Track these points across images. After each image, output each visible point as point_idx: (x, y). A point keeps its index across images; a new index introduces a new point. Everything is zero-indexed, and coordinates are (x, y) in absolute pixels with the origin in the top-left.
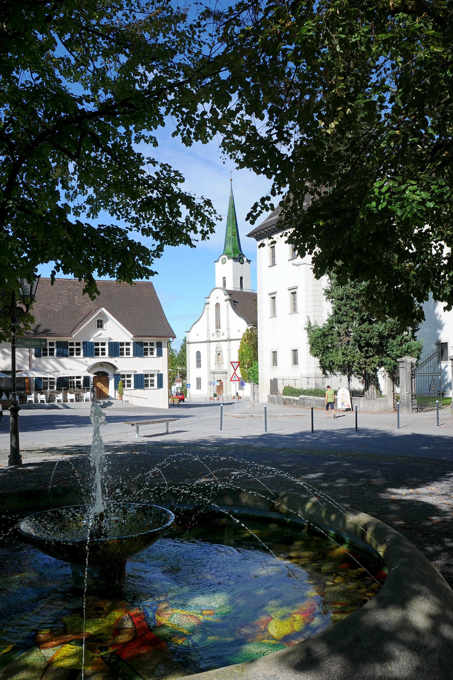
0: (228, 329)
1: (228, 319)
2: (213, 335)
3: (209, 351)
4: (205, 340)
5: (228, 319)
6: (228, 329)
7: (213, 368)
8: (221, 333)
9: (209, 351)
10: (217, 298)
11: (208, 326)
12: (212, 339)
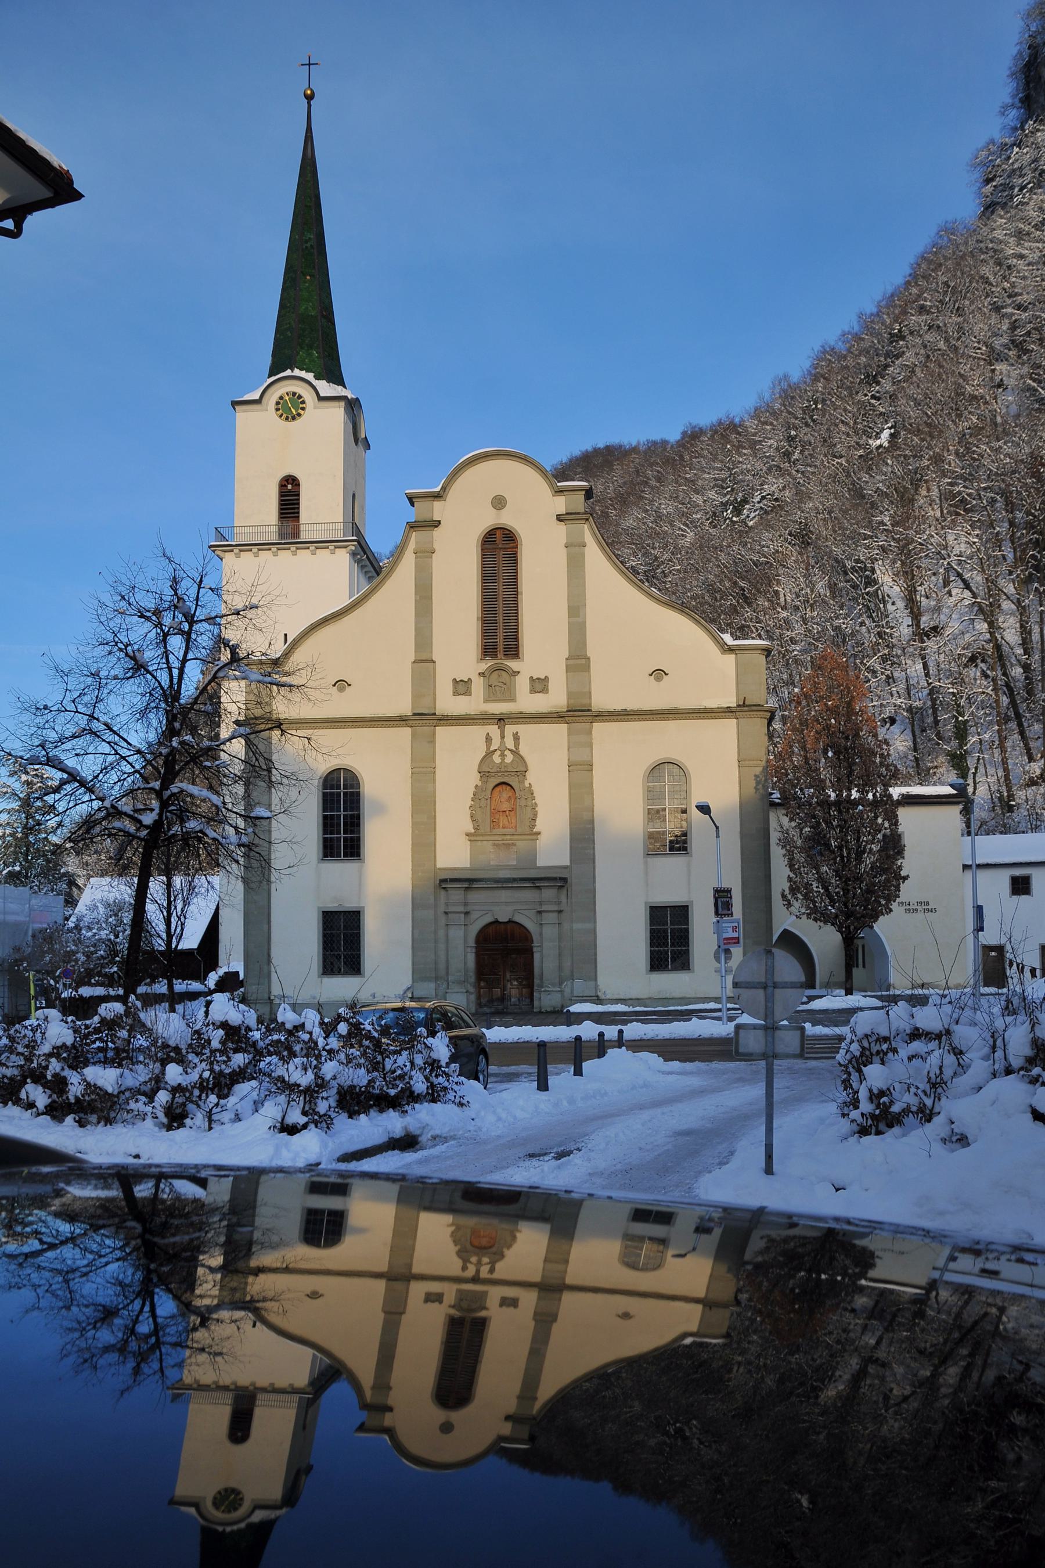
0: (578, 662)
1: (576, 609)
2: (461, 687)
3: (423, 772)
4: (404, 706)
5: (576, 609)
6: (578, 662)
7: (454, 853)
8: (522, 684)
9: (423, 772)
10: (499, 503)
11: (423, 638)
12: (447, 703)
